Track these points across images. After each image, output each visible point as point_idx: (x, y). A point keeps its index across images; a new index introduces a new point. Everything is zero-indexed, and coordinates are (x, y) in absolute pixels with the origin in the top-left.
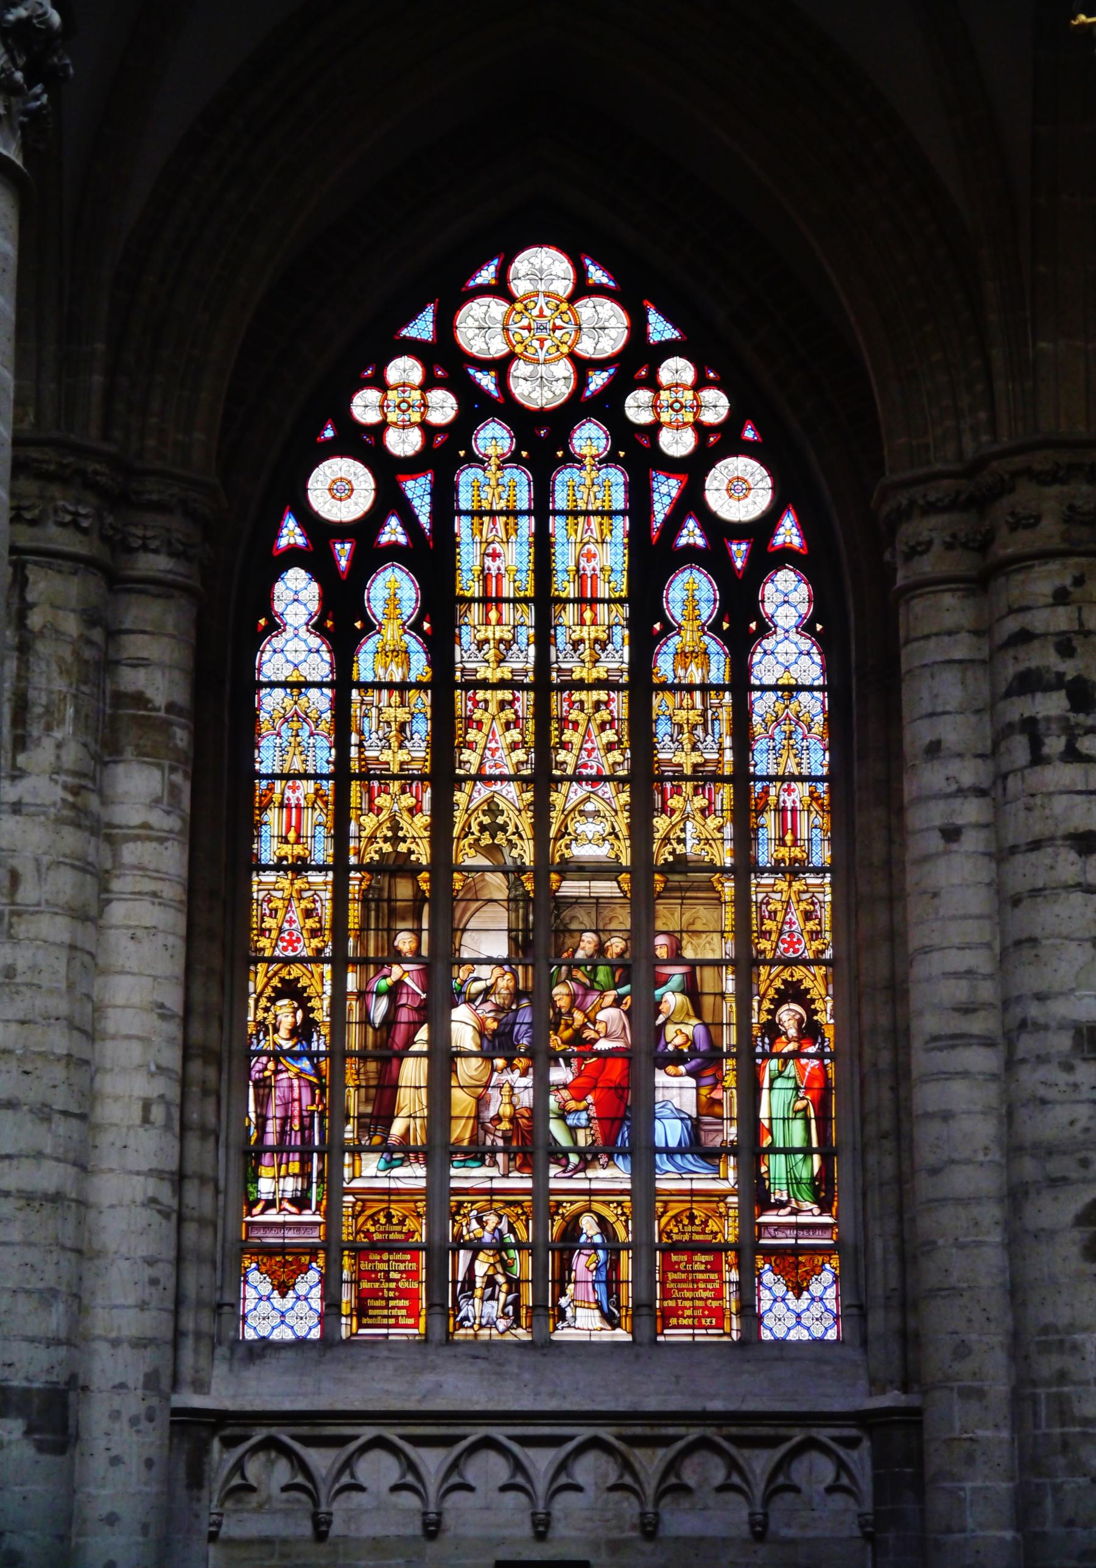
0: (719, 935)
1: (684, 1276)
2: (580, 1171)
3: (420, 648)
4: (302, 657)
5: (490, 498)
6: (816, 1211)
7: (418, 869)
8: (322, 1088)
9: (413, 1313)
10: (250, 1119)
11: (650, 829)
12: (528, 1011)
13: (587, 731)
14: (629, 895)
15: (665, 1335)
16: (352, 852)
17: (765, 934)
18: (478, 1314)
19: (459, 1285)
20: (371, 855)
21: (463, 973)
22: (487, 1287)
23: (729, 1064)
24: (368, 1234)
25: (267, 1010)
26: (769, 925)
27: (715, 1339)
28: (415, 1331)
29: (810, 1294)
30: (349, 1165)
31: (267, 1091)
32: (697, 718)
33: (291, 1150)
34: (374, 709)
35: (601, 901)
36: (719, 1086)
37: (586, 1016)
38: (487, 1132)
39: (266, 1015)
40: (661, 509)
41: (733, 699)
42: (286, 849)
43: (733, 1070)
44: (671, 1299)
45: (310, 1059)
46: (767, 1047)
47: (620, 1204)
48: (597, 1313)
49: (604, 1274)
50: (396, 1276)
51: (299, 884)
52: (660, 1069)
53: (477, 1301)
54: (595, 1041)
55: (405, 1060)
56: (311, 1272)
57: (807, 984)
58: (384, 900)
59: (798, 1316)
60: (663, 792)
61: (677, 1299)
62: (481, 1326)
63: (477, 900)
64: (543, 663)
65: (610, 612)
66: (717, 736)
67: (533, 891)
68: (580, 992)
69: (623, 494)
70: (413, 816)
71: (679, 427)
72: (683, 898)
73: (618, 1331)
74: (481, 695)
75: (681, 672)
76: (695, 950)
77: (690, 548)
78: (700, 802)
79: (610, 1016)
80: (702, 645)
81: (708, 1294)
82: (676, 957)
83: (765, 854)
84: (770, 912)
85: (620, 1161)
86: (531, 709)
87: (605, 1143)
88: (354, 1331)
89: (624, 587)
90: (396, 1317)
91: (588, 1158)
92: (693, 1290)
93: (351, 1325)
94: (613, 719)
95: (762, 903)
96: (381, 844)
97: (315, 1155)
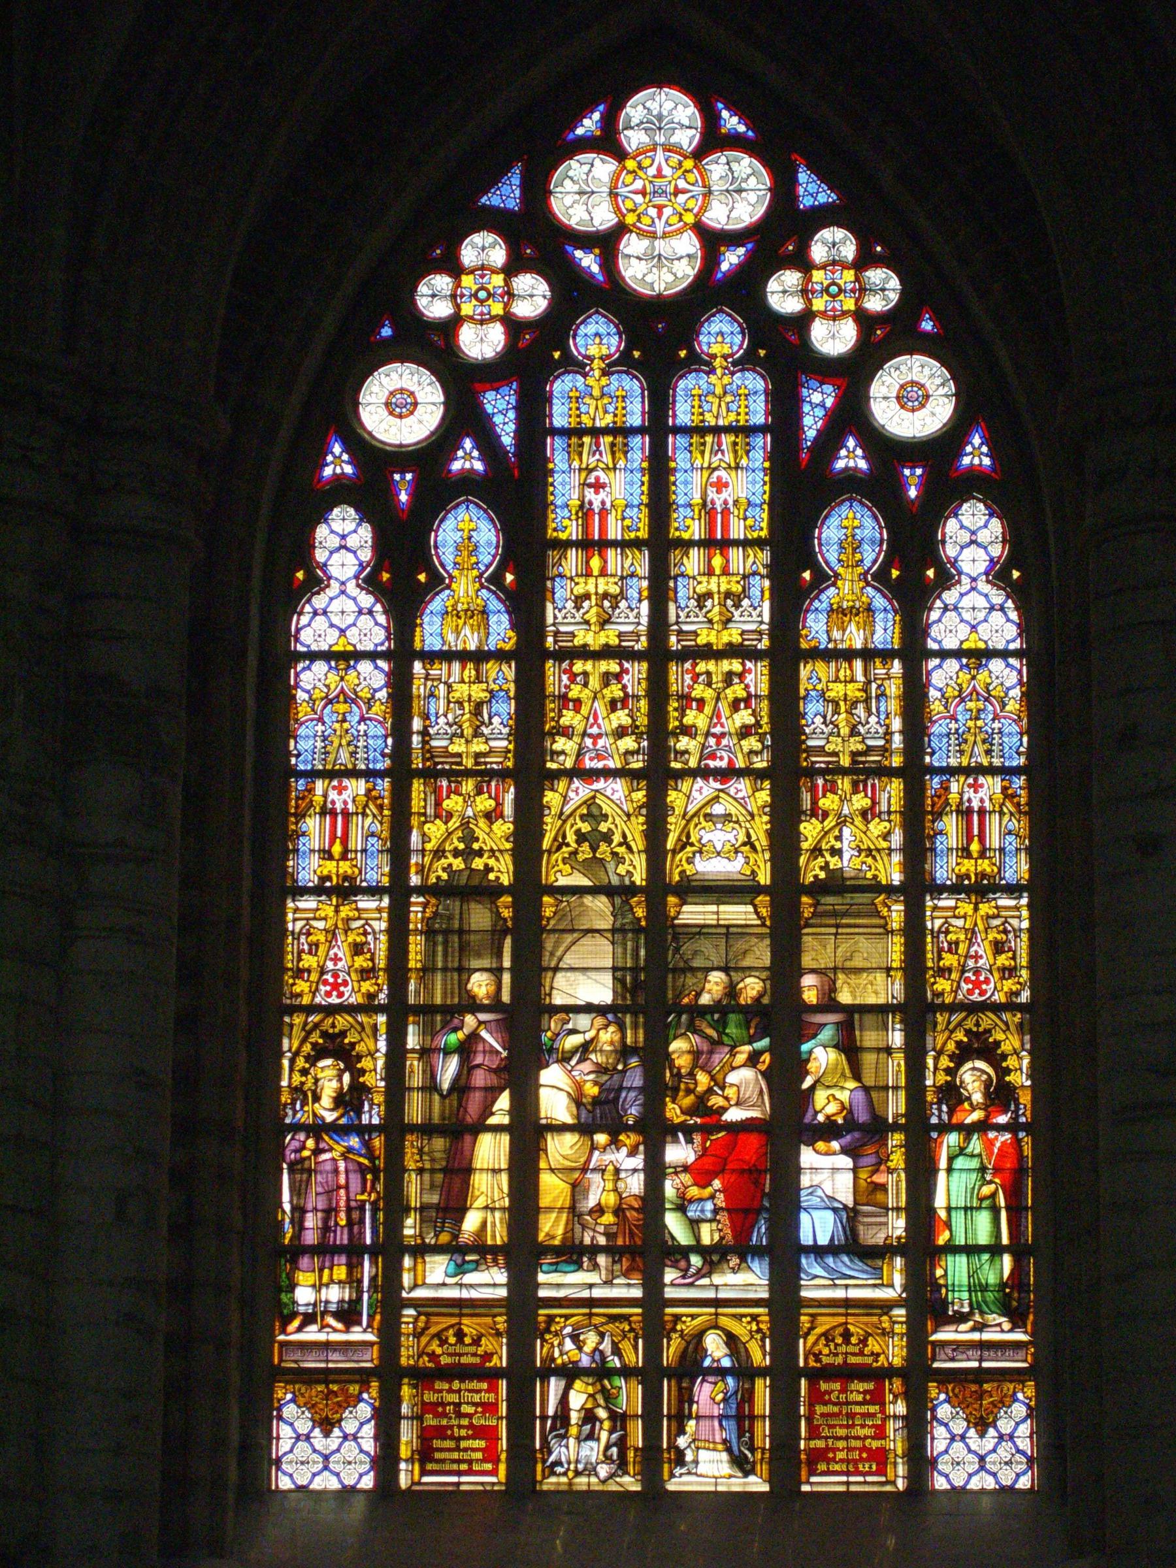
1: (836, 1409)
2: (703, 1276)
3: (501, 607)
4: (350, 620)
5: (592, 411)
7: (498, 890)
9: (491, 1455)
10: (284, 1212)
11: (795, 837)
13: (717, 714)
14: (768, 923)
16: (413, 870)
17: (943, 972)
18: (572, 1458)
19: (549, 1422)
20: (439, 873)
24: (433, 1356)
25: (304, 1072)
26: (949, 960)
28: (493, 1479)
29: (998, 1431)
30: (409, 1270)
31: (305, 1176)
32: (859, 694)
33: (336, 1250)
34: (442, 686)
35: (732, 930)
36: (883, 1167)
37: (713, 1078)
38: (584, 1227)
39: (303, 1079)
40: (812, 424)
41: (903, 668)
42: (330, 867)
43: (901, 1147)
44: (820, 1438)
46: (945, 1117)
47: (754, 1318)
48: (724, 1456)
49: (734, 1406)
51: (345, 911)
53: (572, 1441)
54: (724, 1110)
56: (362, 1405)
59: (982, 1459)
60: (813, 789)
61: (826, 1438)
62: (578, 1473)
63: (573, 931)
64: (659, 624)
65: (745, 557)
66: (883, 717)
68: (705, 1048)
69: (763, 405)
70: (492, 823)
71: (835, 317)
72: (837, 926)
74: (578, 666)
75: (836, 635)
76: (853, 994)
77: (850, 475)
78: (861, 801)
79: (743, 1078)
80: (864, 599)
81: (866, 1432)
82: (829, 1004)
83: (944, 869)
84: (950, 944)
85: (756, 1265)
86: (644, 684)
88: (416, 1478)
89: (764, 525)
90: (470, 1462)
91: (715, 1257)
92: (847, 1426)
93: (412, 1472)
94: (749, 695)
95: (939, 932)
96: (451, 860)
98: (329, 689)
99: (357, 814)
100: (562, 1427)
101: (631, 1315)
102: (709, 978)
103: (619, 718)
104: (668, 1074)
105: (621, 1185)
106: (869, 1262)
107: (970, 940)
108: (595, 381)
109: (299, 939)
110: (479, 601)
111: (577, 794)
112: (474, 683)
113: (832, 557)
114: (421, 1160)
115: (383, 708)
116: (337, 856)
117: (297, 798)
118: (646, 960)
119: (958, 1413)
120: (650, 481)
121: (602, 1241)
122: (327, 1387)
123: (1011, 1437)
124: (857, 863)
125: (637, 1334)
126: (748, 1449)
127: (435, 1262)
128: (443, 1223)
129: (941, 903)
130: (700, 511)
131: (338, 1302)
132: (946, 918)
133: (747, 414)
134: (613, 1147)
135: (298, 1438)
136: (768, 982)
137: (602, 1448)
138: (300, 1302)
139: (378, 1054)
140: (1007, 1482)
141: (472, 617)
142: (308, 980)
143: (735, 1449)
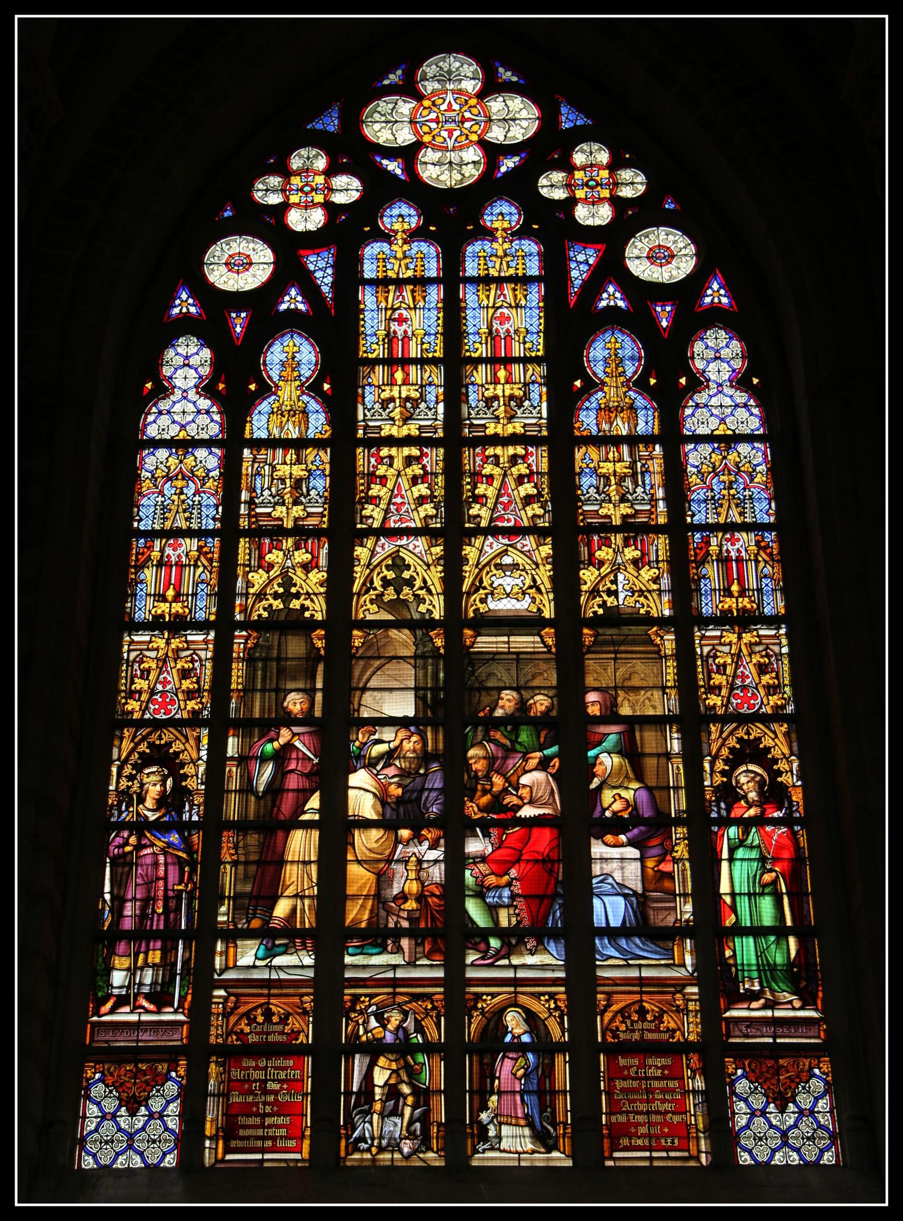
1: (635, 1084)
2: (503, 958)
3: (318, 407)
4: (190, 418)
6: (797, 1004)
7: (313, 624)
10: (104, 901)
11: (578, 581)
12: (439, 775)
14: (554, 650)
15: (615, 1159)
16: (237, 609)
17: (715, 689)
20: (260, 611)
22: (387, 1100)
24: (241, 1034)
25: (131, 778)
26: (718, 679)
27: (679, 1164)
28: (297, 1156)
30: (221, 953)
31: (126, 869)
33: (153, 935)
34: (267, 467)
35: (521, 656)
36: (668, 858)
37: (507, 780)
38: (389, 912)
39: (130, 783)
40: (578, 274)
41: (663, 451)
42: (163, 607)
43: (684, 839)
44: (621, 1113)
45: (181, 834)
46: (724, 813)
47: (552, 996)
48: (527, 1131)
49: (535, 1081)
50: (276, 1086)
51: (175, 643)
52: (597, 838)
53: (375, 1117)
54: (519, 807)
56: (169, 1083)
57: (767, 742)
58: (272, 659)
59: (784, 1134)
60: (589, 544)
61: (627, 1112)
62: (381, 1149)
63: (379, 658)
64: (453, 418)
66: (648, 488)
67: (444, 647)
68: (500, 755)
69: (537, 263)
70: (308, 572)
72: (616, 652)
73: (555, 1154)
74: (384, 452)
75: (605, 426)
76: (632, 707)
78: (631, 553)
81: (667, 1106)
85: (552, 947)
86: (441, 464)
88: (220, 1156)
89: (541, 347)
90: (274, 1139)
92: (648, 1101)
93: (216, 1149)
94: (532, 473)
95: (708, 656)
96: (271, 601)
98: (169, 470)
99: (190, 565)
100: (365, 1104)
101: (434, 994)
102: (502, 695)
103: (419, 491)
104: (466, 777)
105: (423, 874)
107: (737, 663)
108: (398, 249)
109: (132, 666)
110: (300, 404)
111: (383, 549)
112: (295, 464)
113: (599, 369)
114: (236, 853)
115: (216, 484)
116: (170, 598)
117: (137, 554)
118: (444, 681)
119: (756, 1088)
120: (444, 317)
121: (405, 924)
122: (136, 1066)
123: (812, 1112)
124: (630, 601)
125: (439, 1011)
126: (550, 1124)
127: (243, 946)
128: (255, 910)
129: (708, 634)
130: (486, 338)
131: (151, 985)
132: (713, 645)
133: (524, 269)
134: (416, 840)
135: (103, 1117)
136: (555, 700)
137: (405, 1124)
138: (115, 985)
139: (200, 762)
140: (811, 1158)
141: (293, 416)
142: (139, 700)
143: (537, 1123)
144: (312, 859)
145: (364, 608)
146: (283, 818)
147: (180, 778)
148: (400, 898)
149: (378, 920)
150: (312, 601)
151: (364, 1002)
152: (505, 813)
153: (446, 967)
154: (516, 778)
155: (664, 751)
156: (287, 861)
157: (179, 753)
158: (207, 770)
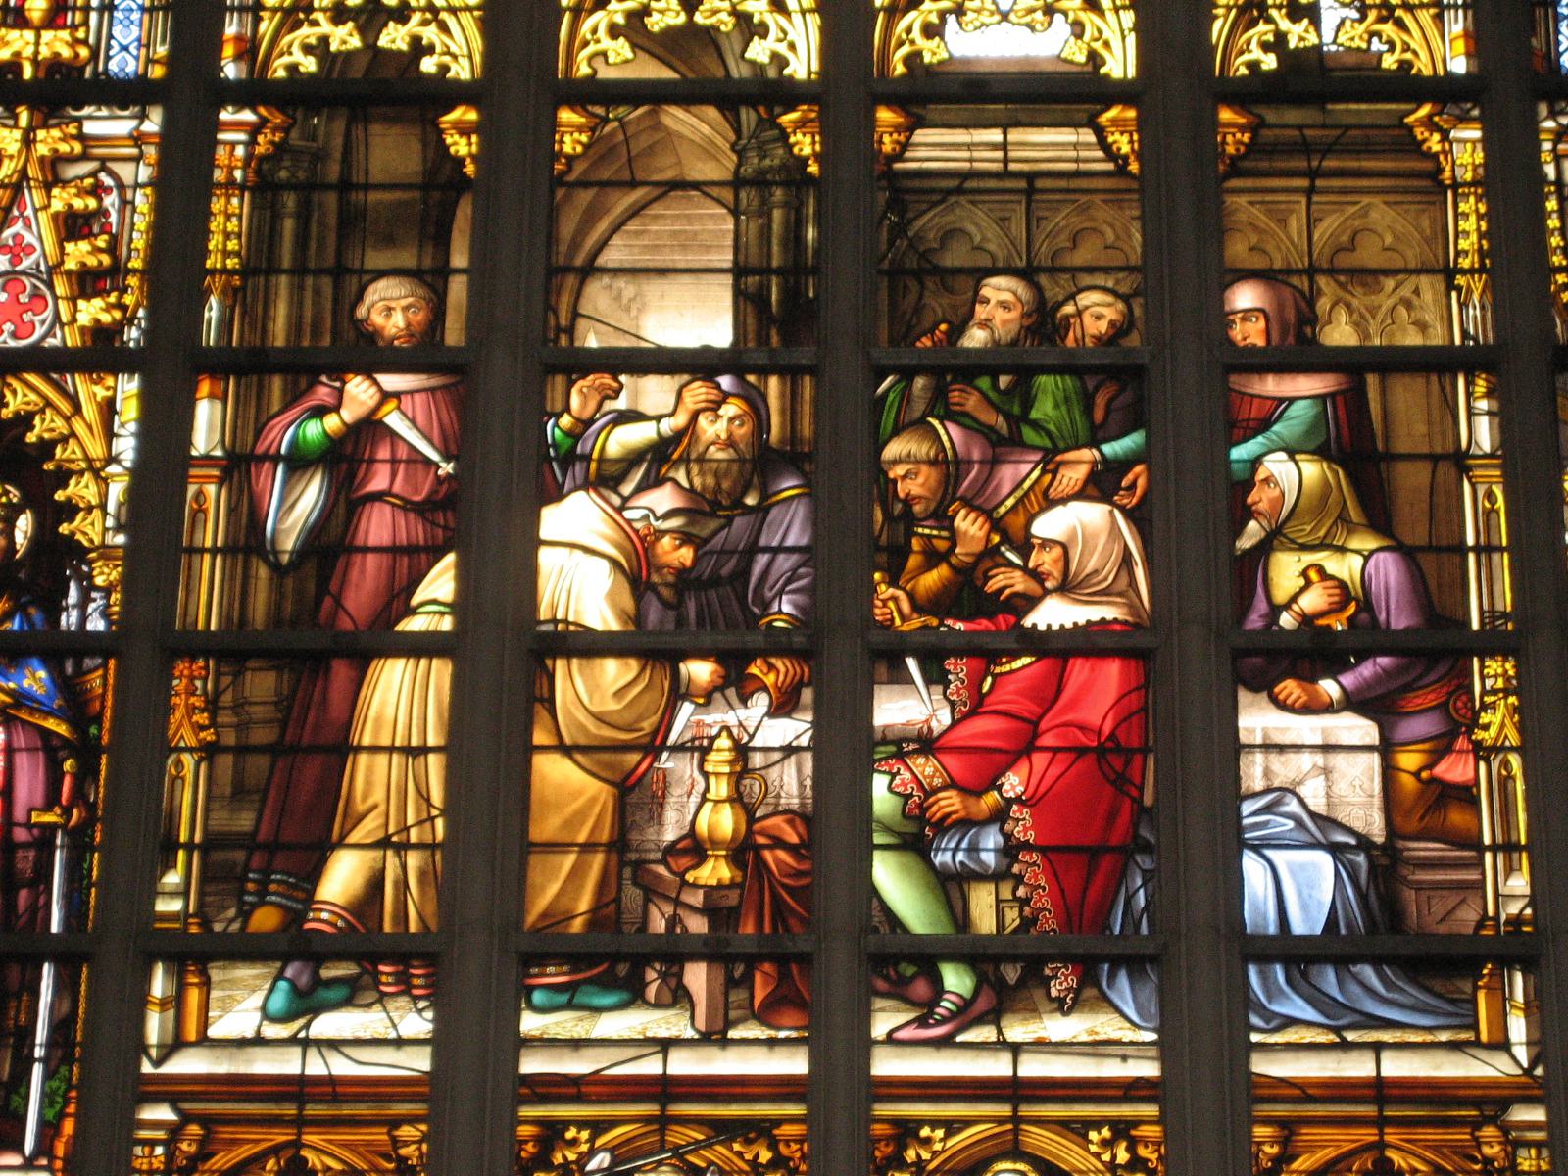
0: (1439, 282)
2: (979, 1021)
7: (446, 93)
8: (86, 751)
12: (799, 512)
14: (1134, 167)
16: (229, 51)
20: (294, 57)
21: (580, 398)
23: (1492, 672)
30: (163, 1004)
35: (1040, 184)
36: (1461, 743)
37: (996, 525)
38: (652, 891)
43: (1507, 692)
47: (1122, 1130)
51: (48, 141)
52: (1255, 688)
54: (1031, 602)
55: (377, 665)
58: (328, 187)
63: (633, 184)
67: (817, 156)
68: (976, 455)
72: (1313, 174)
76: (1359, 326)
85: (1123, 991)
87: (1070, 918)
96: (326, 27)
97: (47, 971)
101: (779, 1122)
102: (985, 292)
106: (1437, 986)
114: (213, 724)
118: (817, 252)
121: (697, 925)
124: (1354, 36)
127: (232, 983)
139: (113, 469)
144: (432, 741)
145: (592, 48)
146: (346, 624)
147: (53, 514)
148: (685, 851)
149: (619, 911)
150: (444, 28)
151: (574, 1142)
152: (990, 616)
153: (812, 1042)
154: (1021, 519)
155: (1450, 447)
156: (359, 749)
157: (53, 444)
158: (134, 494)
